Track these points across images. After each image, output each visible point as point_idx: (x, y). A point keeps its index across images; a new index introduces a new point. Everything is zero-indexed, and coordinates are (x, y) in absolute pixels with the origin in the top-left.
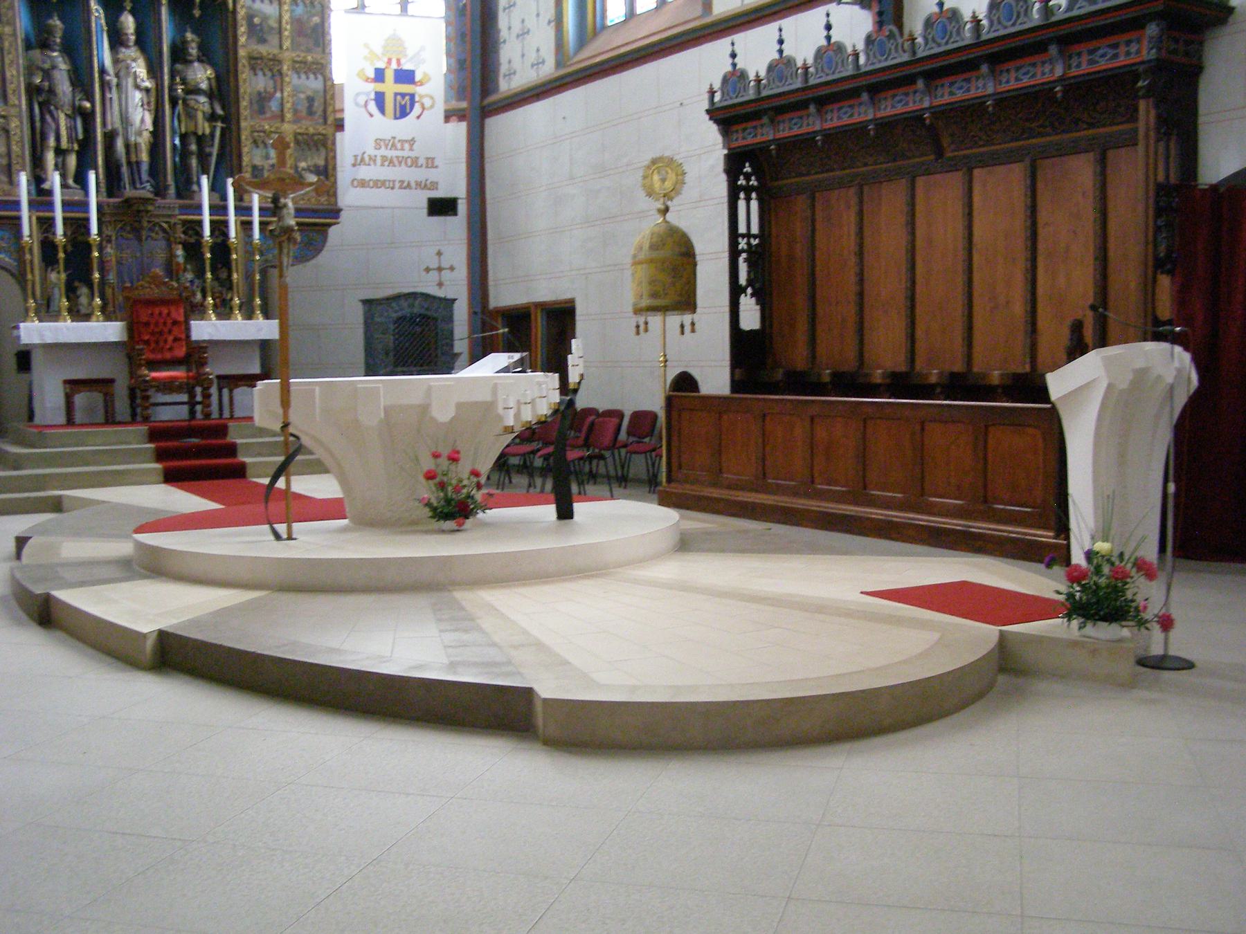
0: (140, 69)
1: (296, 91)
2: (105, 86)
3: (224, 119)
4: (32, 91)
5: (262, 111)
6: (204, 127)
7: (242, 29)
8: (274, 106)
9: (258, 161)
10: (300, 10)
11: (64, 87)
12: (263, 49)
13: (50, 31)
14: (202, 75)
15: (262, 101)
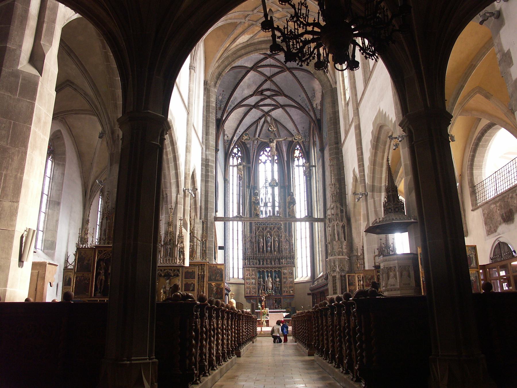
0: (271, 280)
1: (289, 281)
2: (266, 282)
3: (280, 285)
4: (258, 283)
5: (285, 284)
6: (278, 286)
7: (282, 274)
8: (286, 283)
9: (284, 290)
10: (289, 271)
11: (262, 283)
12: (285, 276)
13: (261, 276)
14: (278, 280)
15: (285, 282)
